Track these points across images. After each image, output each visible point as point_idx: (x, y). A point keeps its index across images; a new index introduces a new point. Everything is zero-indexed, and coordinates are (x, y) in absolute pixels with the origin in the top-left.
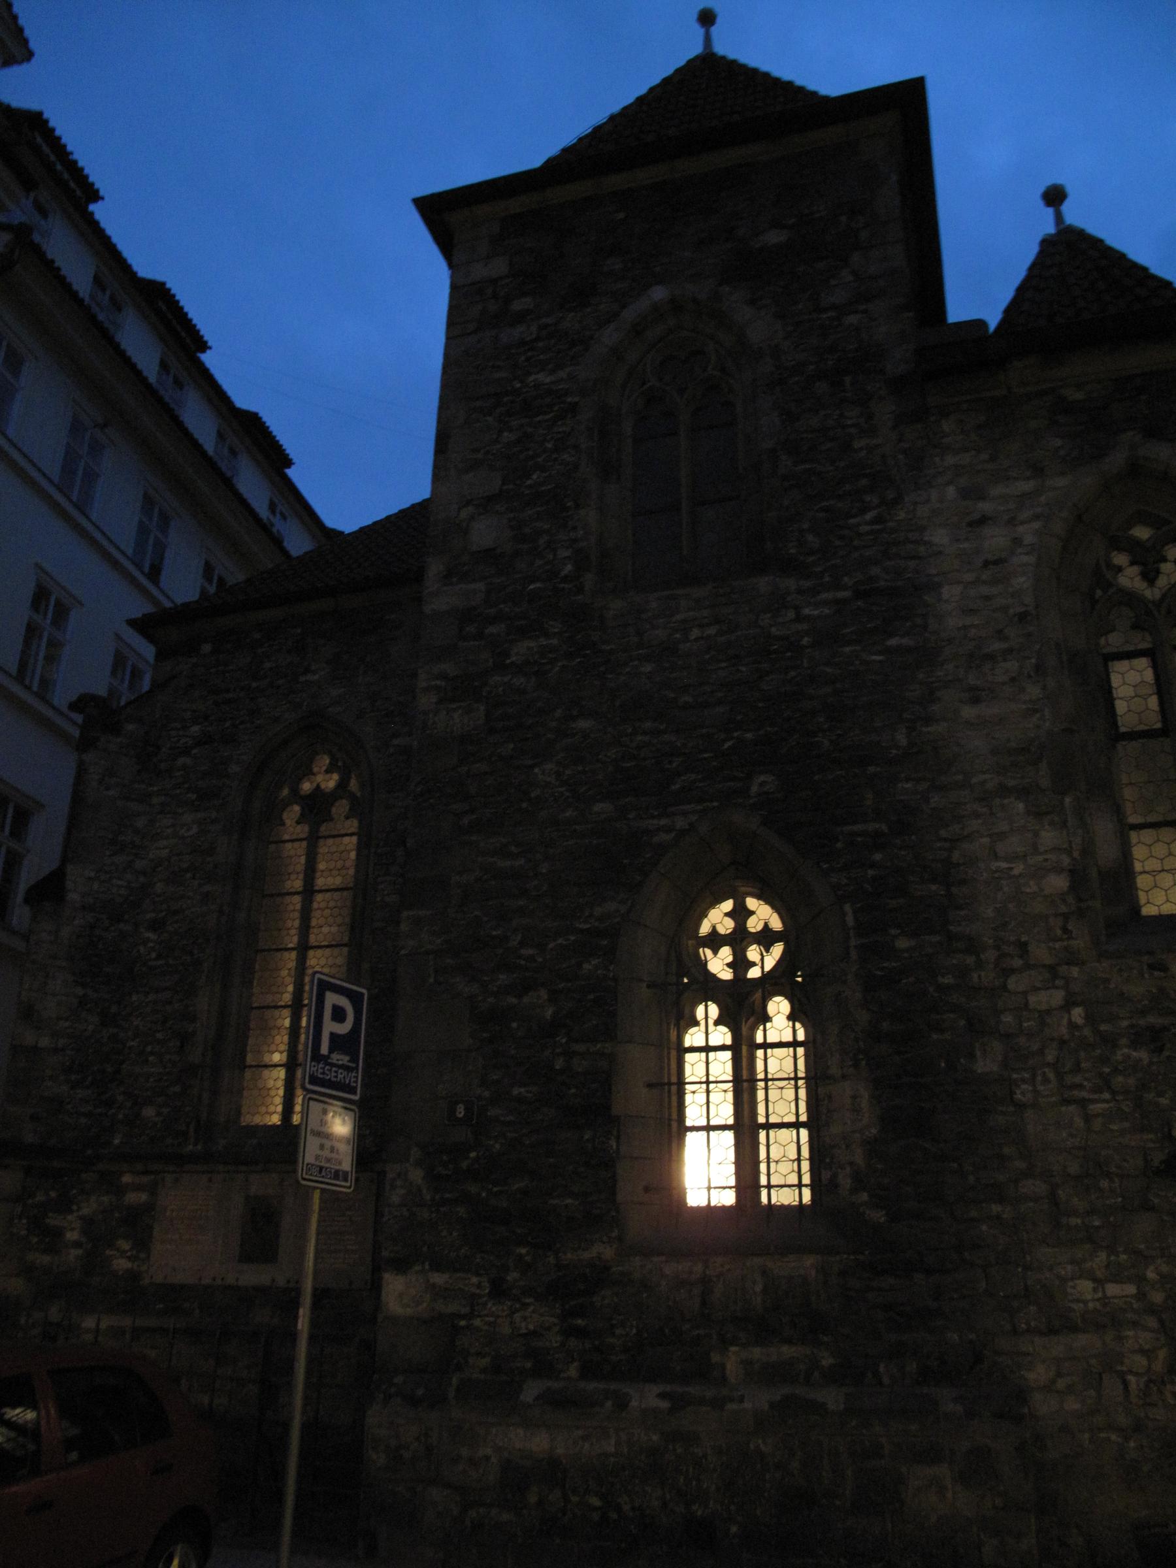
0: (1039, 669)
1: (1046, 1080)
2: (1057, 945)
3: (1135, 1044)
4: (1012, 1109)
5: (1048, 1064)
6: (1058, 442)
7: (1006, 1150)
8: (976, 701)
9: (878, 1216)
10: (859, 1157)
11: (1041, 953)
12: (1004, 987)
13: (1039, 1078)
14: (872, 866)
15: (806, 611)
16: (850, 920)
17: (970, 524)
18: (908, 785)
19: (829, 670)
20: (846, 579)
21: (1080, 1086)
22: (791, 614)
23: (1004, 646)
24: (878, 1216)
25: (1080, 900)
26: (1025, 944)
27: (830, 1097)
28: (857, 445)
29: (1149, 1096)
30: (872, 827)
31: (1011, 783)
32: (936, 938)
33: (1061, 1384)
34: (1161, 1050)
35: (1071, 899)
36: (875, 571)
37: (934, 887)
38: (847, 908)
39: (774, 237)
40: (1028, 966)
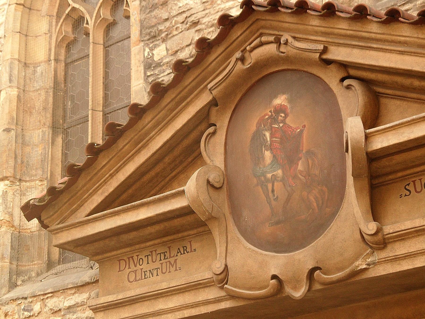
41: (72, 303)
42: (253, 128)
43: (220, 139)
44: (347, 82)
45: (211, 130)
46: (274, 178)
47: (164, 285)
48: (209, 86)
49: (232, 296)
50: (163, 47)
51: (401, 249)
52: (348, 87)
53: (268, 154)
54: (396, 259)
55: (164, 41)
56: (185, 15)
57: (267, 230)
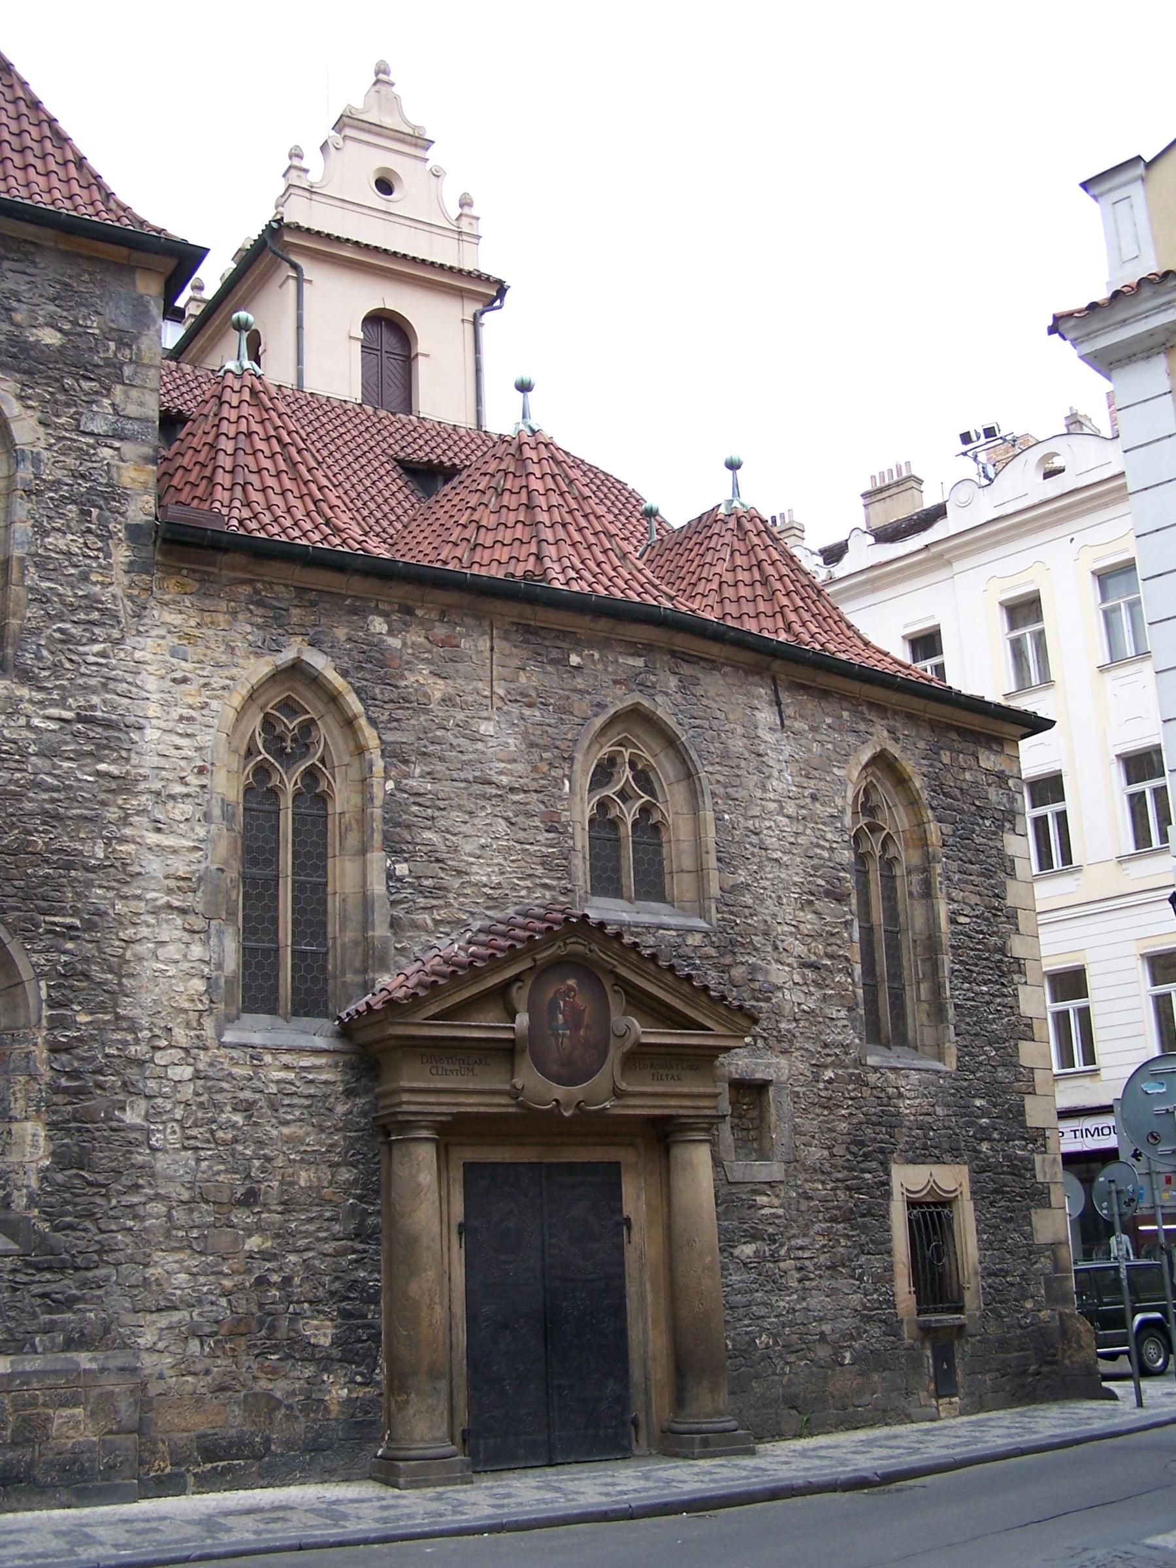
0: (207, 817)
1: (174, 1132)
2: (192, 1033)
3: (235, 1110)
4: (148, 1151)
5: (176, 1120)
6: (249, 628)
7: (141, 1182)
8: (159, 830)
9: (45, 1227)
10: (34, 1183)
11: (181, 1035)
12: (152, 1060)
13: (169, 1130)
14: (65, 952)
15: (36, 722)
16: (44, 994)
17: (174, 680)
18: (99, 891)
19: (49, 780)
20: (70, 700)
21: (195, 1138)
22: (22, 721)
23: (184, 790)
24: (45, 1227)
25: (212, 1001)
26: (170, 1029)
27: (10, 1132)
28: (94, 578)
29: (240, 1148)
30: (68, 920)
31: (176, 903)
32: (107, 1017)
33: (160, 1345)
34: (251, 1116)
35: (205, 999)
36: (95, 700)
37: (109, 976)
38: (43, 984)
39: (50, 337)
40: (171, 1046)
41: (308, 1064)
42: (551, 994)
43: (525, 992)
44: (616, 988)
45: (520, 984)
46: (564, 1035)
47: (471, 1086)
48: (538, 957)
49: (519, 1105)
50: (405, 865)
51: (631, 1102)
52: (616, 992)
53: (560, 1016)
54: (628, 1106)
55: (406, 860)
56: (429, 848)
57: (554, 1068)
